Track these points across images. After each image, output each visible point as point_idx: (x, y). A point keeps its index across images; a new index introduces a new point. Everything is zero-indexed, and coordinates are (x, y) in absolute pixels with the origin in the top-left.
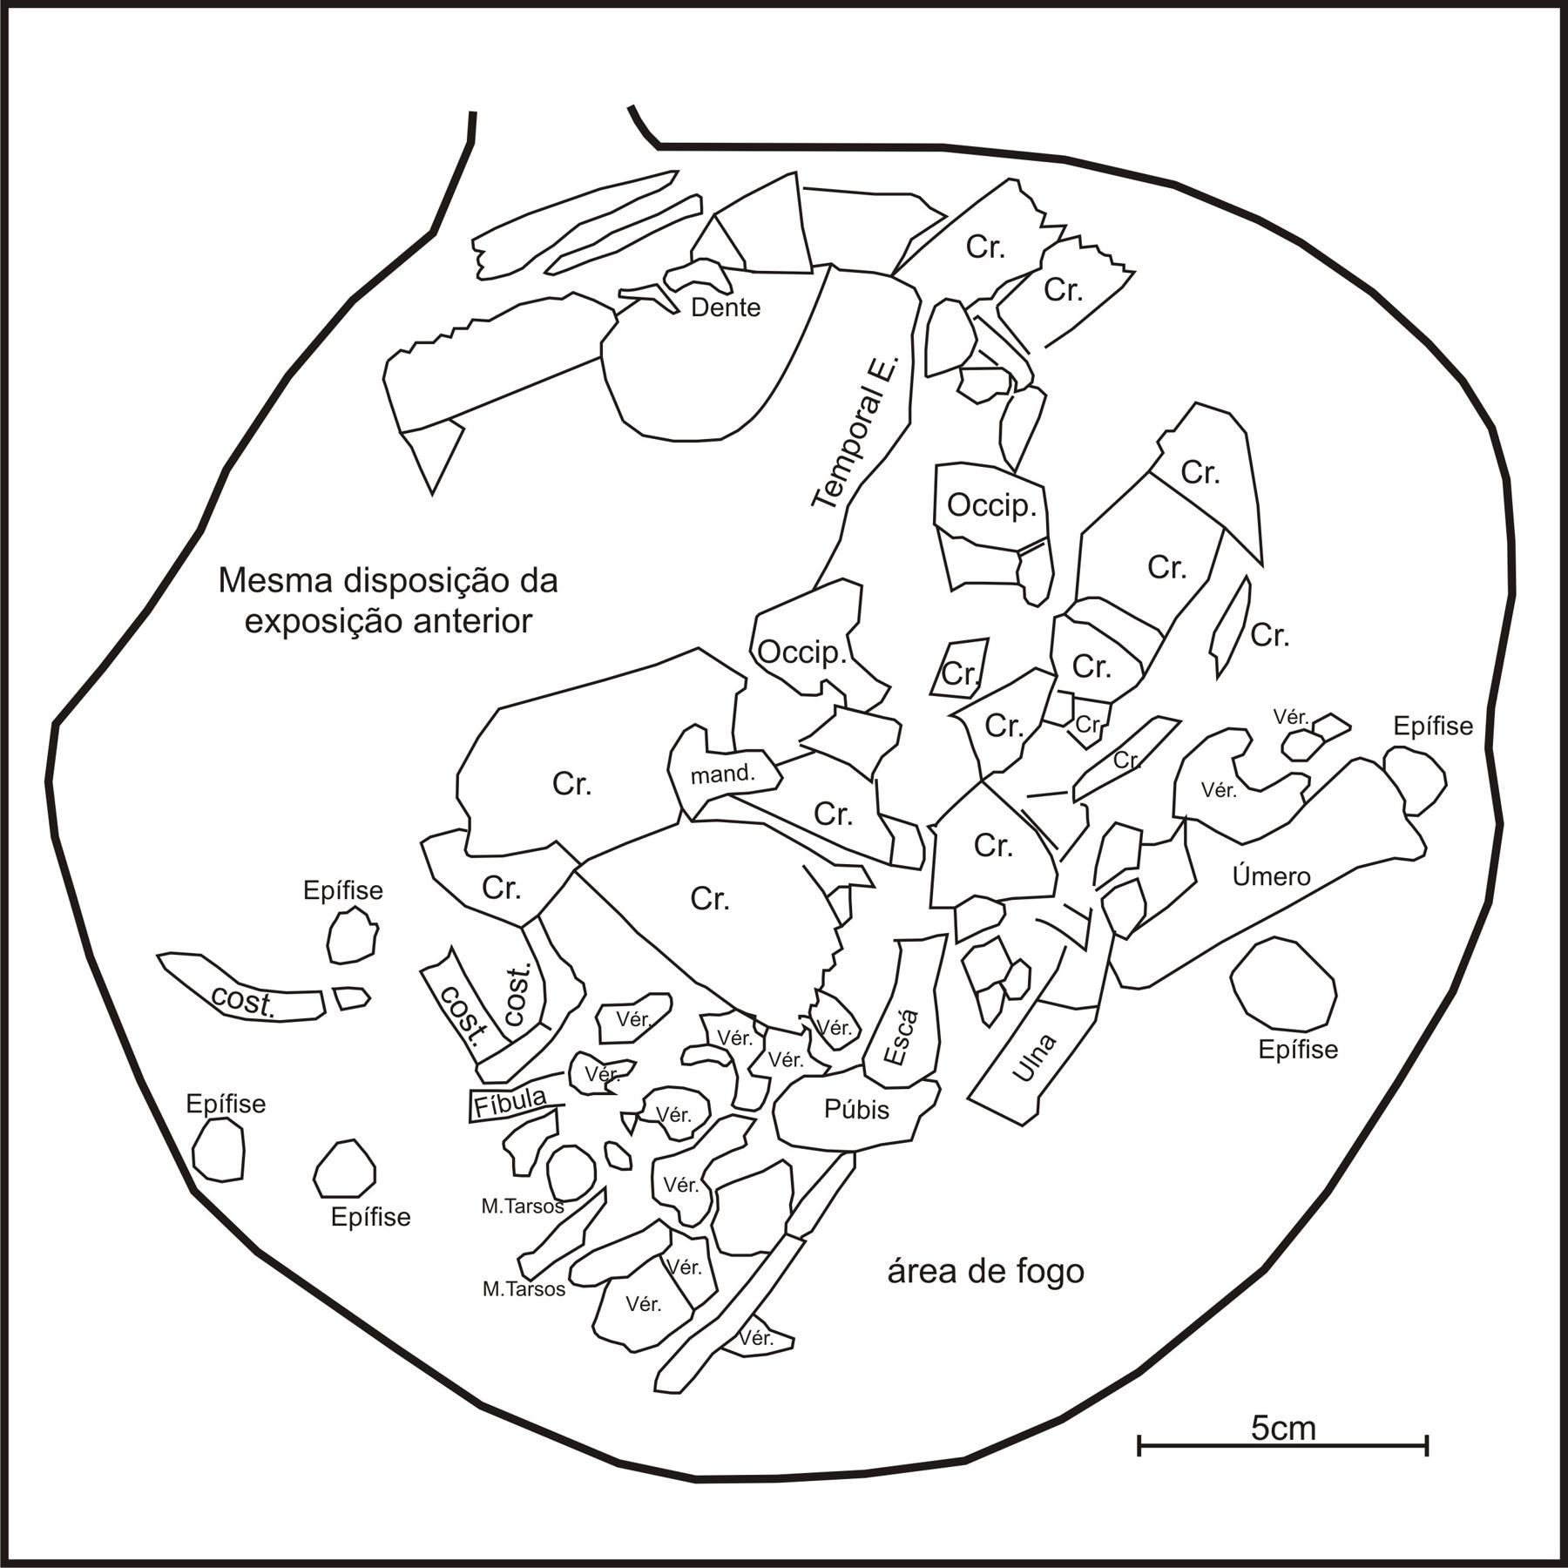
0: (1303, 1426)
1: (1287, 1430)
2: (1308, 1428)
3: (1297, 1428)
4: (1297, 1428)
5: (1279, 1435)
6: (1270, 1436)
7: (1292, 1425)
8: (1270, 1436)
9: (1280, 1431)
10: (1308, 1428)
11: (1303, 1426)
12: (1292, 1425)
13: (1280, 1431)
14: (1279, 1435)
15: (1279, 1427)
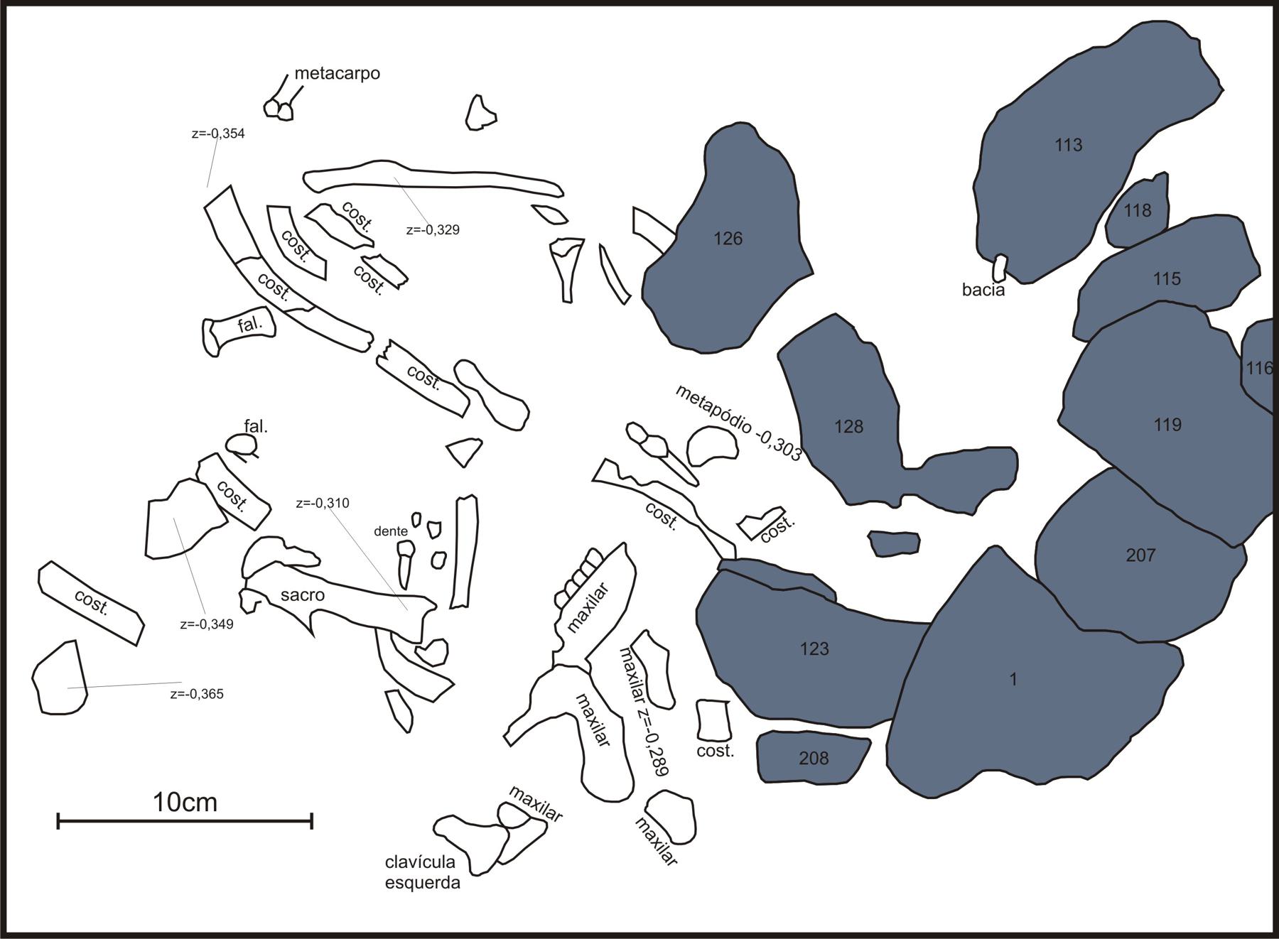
0: (207, 800)
1: (195, 804)
2: (211, 802)
3: (203, 802)
4: (203, 802)
5: (189, 807)
6: (185, 809)
7: (199, 800)
8: (185, 809)
9: (189, 804)
10: (211, 802)
11: (207, 800)
12: (199, 800)
13: (189, 804)
14: (189, 807)
15: (189, 801)
